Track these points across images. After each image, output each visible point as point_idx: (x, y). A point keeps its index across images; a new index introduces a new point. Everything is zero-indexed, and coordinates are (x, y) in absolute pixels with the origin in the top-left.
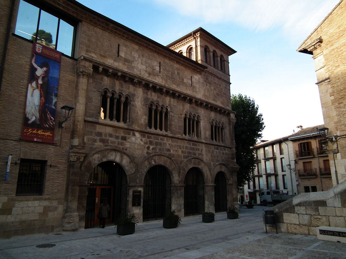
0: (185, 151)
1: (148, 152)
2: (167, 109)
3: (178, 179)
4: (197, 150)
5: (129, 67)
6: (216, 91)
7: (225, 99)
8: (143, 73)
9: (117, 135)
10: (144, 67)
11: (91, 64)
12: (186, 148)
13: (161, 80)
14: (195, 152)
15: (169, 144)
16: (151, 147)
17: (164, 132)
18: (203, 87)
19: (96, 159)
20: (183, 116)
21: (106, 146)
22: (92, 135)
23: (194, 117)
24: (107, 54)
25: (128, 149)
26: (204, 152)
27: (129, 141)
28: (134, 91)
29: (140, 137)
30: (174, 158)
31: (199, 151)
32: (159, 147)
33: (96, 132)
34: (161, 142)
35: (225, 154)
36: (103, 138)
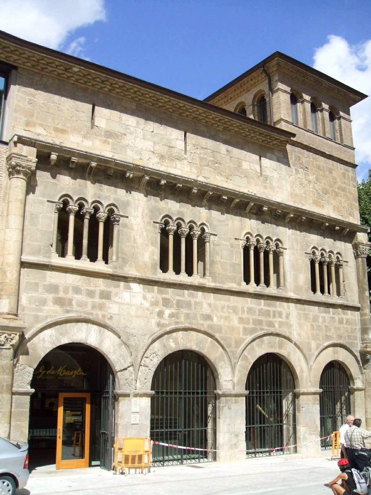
0: (248, 319)
1: (159, 322)
2: (203, 230)
3: (231, 378)
4: (277, 315)
5: (115, 147)
6: (320, 183)
7: (343, 200)
8: (147, 157)
9: (90, 288)
10: (149, 145)
11: (34, 150)
12: (250, 310)
13: (188, 169)
14: (271, 319)
15: (210, 305)
16: (167, 312)
17: (196, 279)
18: (289, 177)
19: (46, 339)
20: (242, 243)
21: (68, 312)
22: (37, 291)
23: (268, 243)
24: (68, 125)
25: (115, 318)
26: (293, 320)
27: (115, 300)
29: (142, 292)
30: (221, 335)
32: (185, 311)
33: (46, 283)
34: (190, 302)
35: (345, 322)
36: (60, 296)
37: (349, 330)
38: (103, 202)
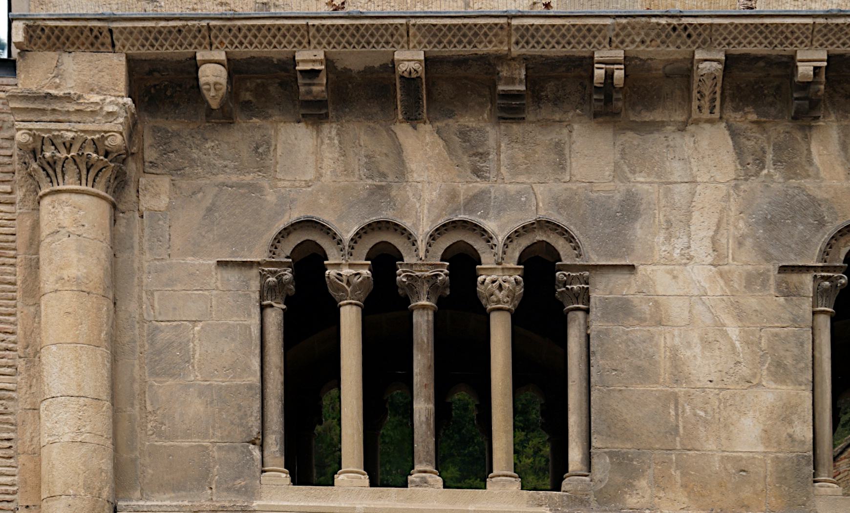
28: (618, 173)
38: (490, 225)
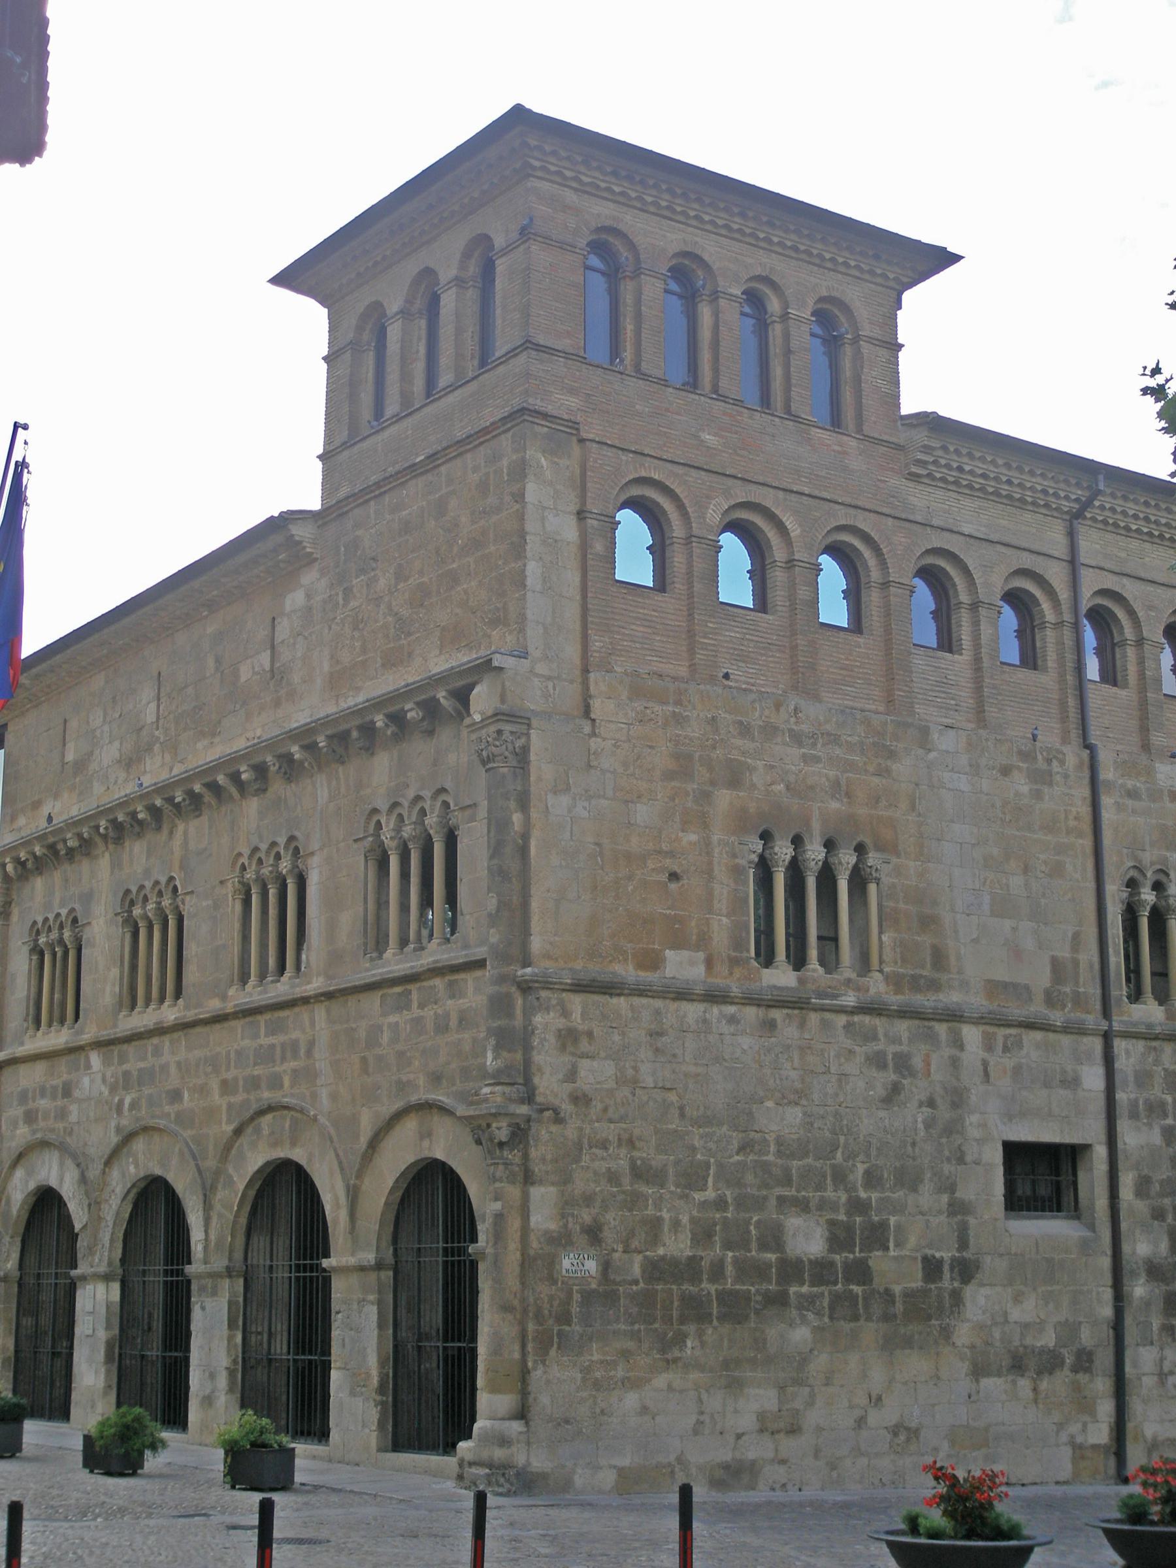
4: (289, 1054)
31: (295, 1055)
35: (453, 1023)
37: (467, 1047)
